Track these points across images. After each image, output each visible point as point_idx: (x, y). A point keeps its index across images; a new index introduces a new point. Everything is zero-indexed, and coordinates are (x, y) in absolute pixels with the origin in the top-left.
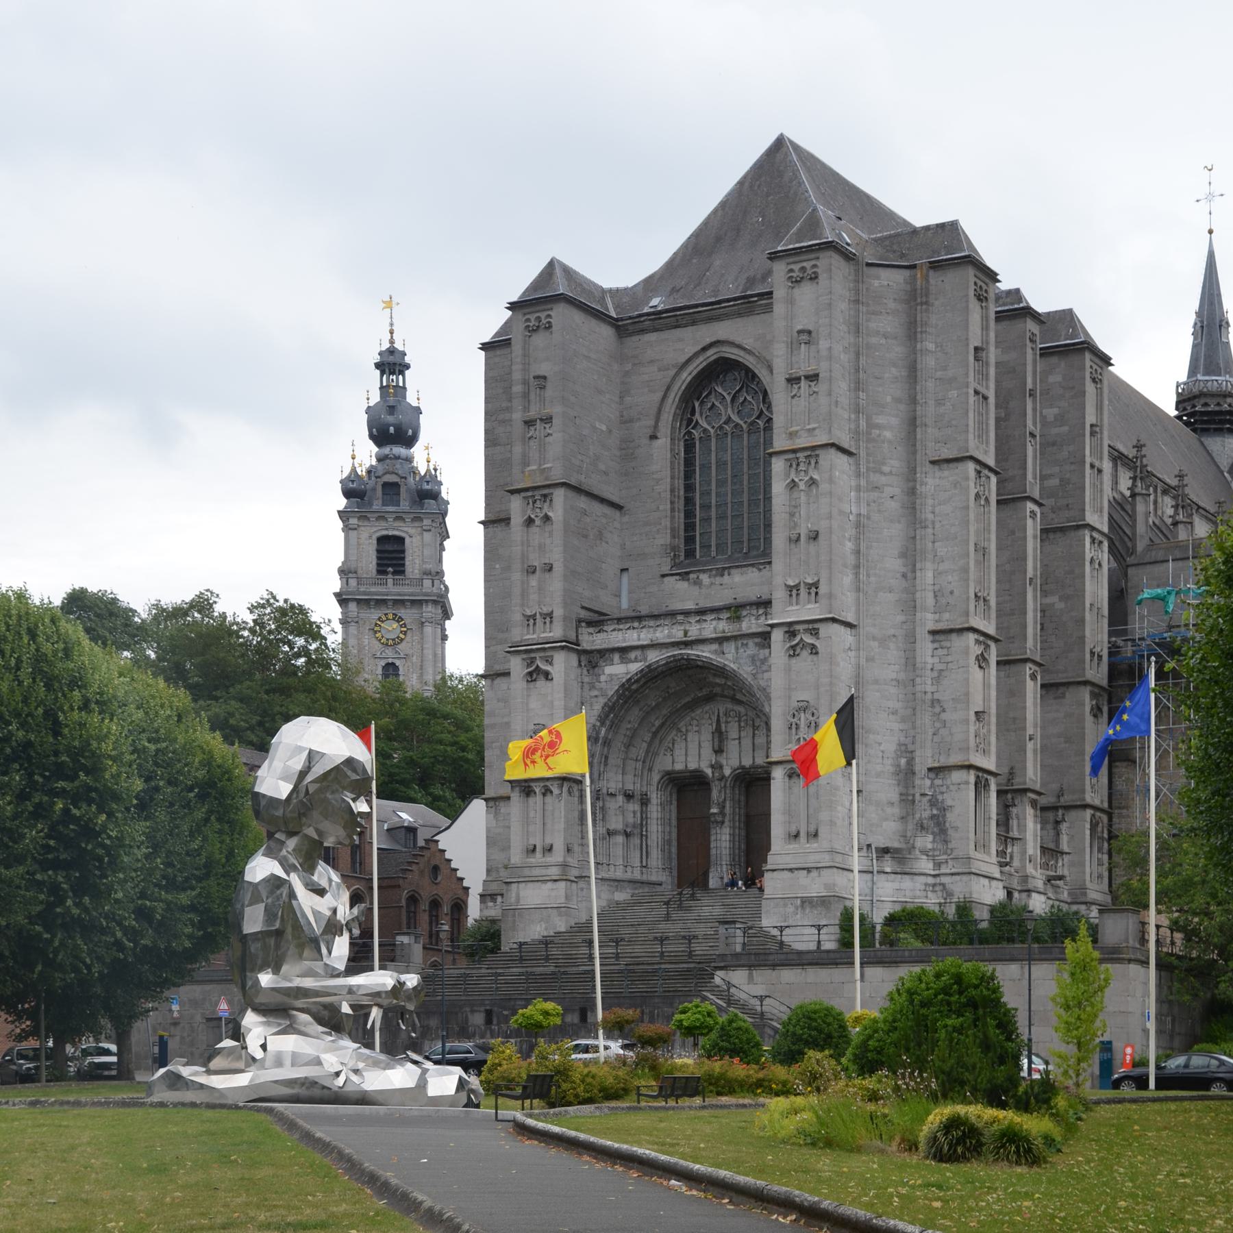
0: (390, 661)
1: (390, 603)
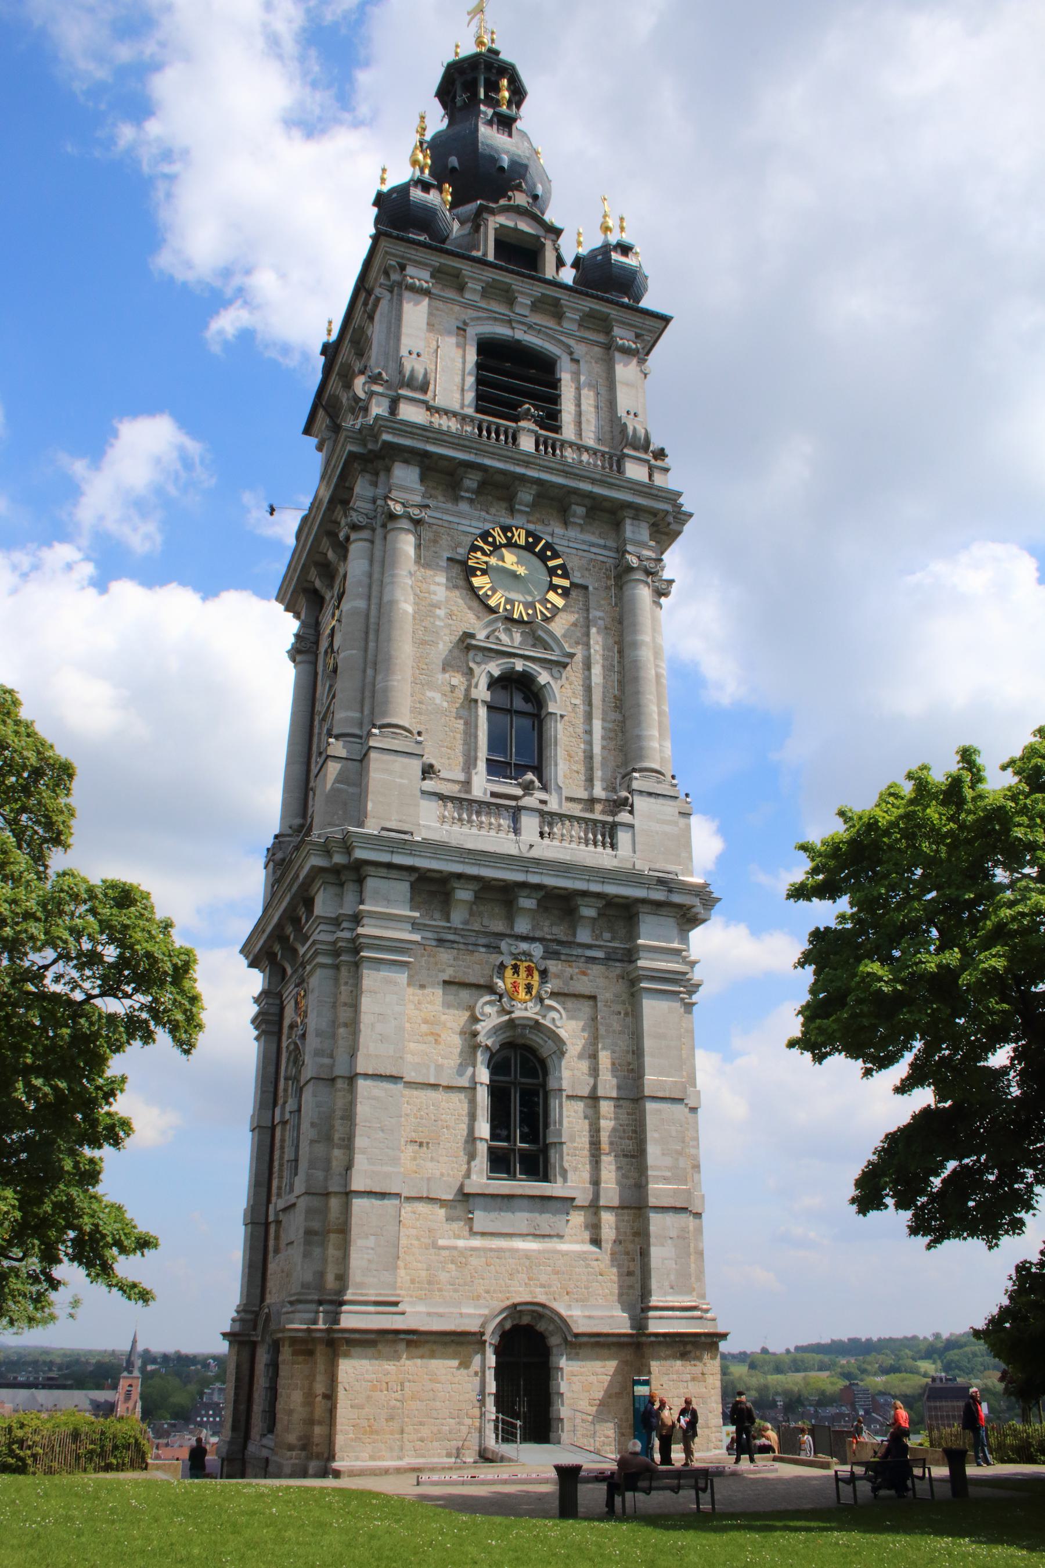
0: (519, 666)
1: (526, 496)
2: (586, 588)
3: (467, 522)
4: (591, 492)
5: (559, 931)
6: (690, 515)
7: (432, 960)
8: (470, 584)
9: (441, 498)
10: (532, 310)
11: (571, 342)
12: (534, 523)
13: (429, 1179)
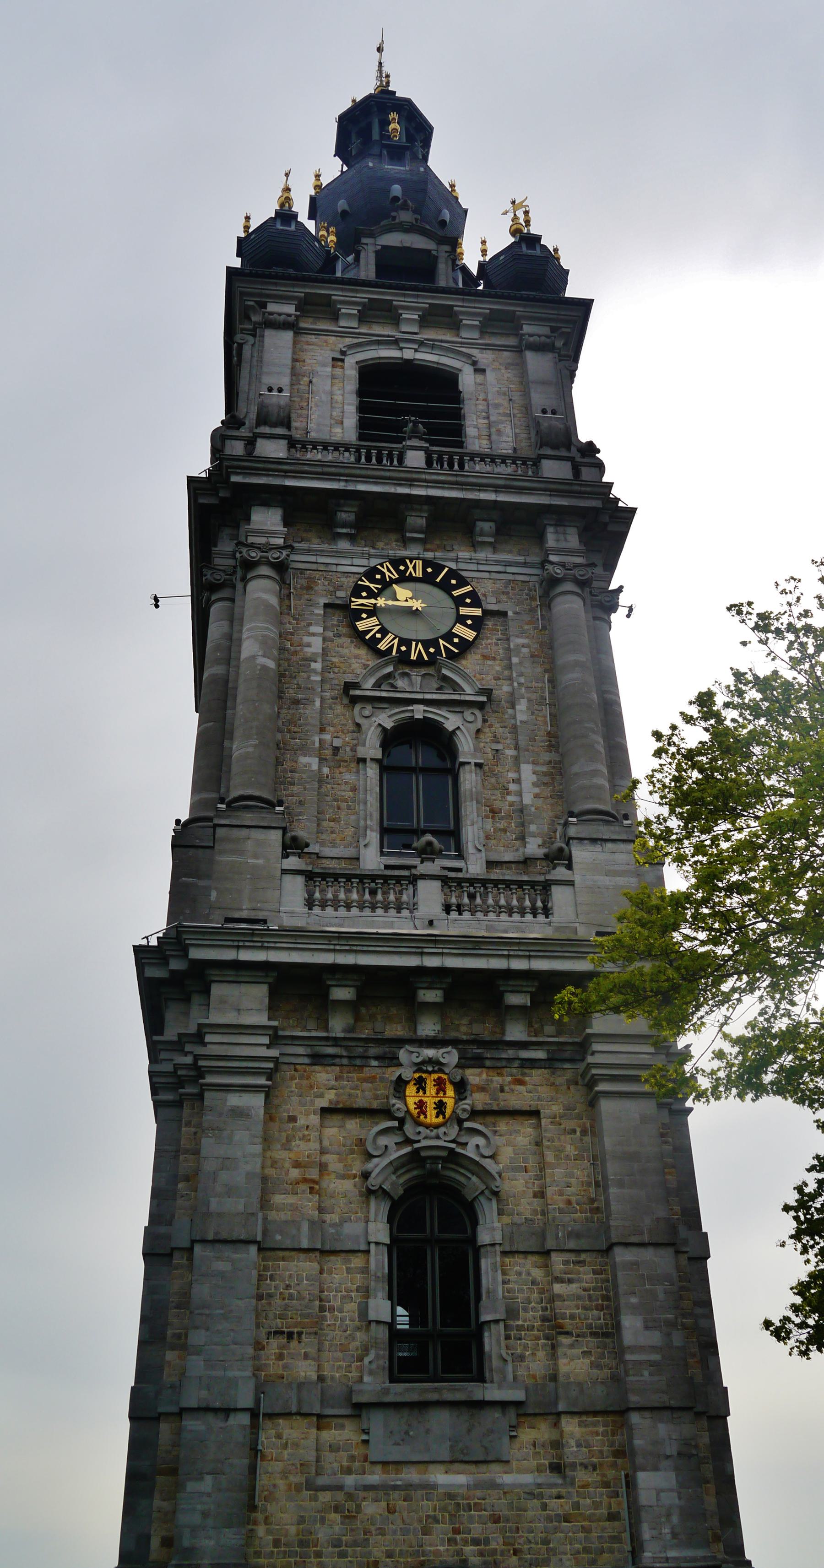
0: (419, 712)
1: (417, 520)
2: (504, 614)
3: (348, 562)
4: (496, 502)
5: (484, 1030)
6: (633, 511)
7: (305, 1082)
8: (355, 628)
9: (317, 541)
10: (421, 327)
11: (474, 352)
12: (432, 551)
13: (301, 1385)
